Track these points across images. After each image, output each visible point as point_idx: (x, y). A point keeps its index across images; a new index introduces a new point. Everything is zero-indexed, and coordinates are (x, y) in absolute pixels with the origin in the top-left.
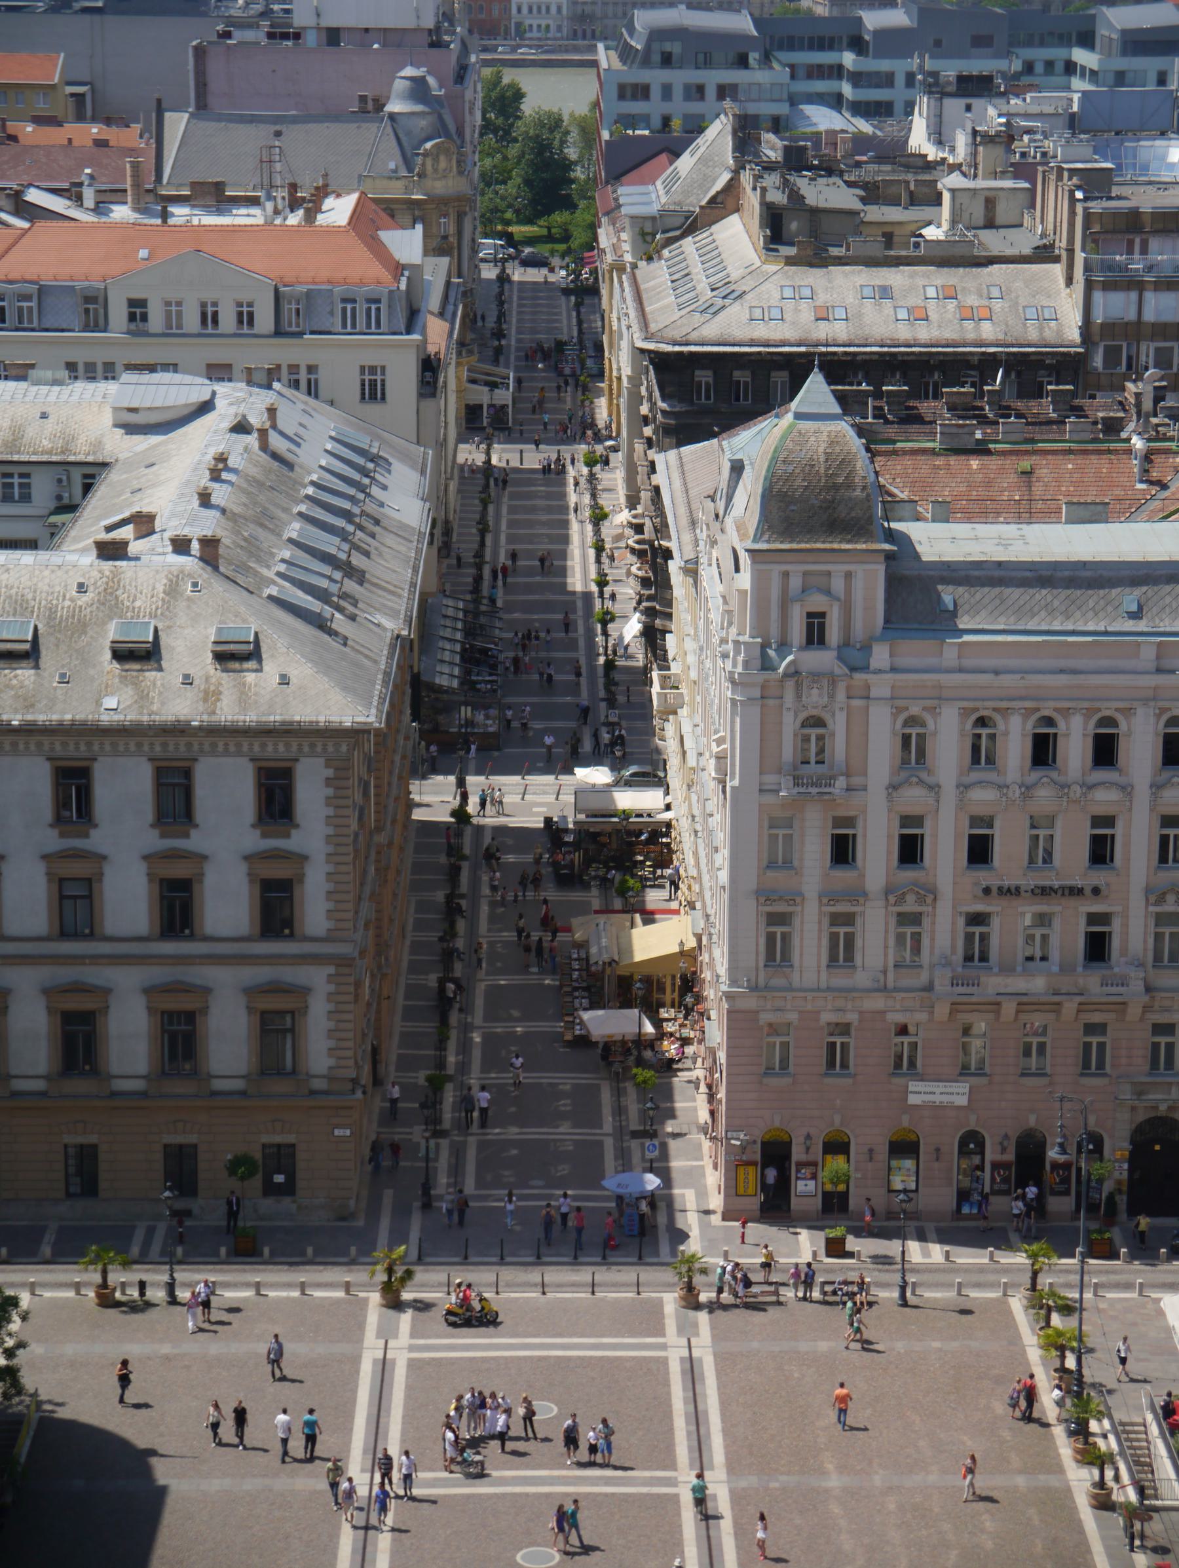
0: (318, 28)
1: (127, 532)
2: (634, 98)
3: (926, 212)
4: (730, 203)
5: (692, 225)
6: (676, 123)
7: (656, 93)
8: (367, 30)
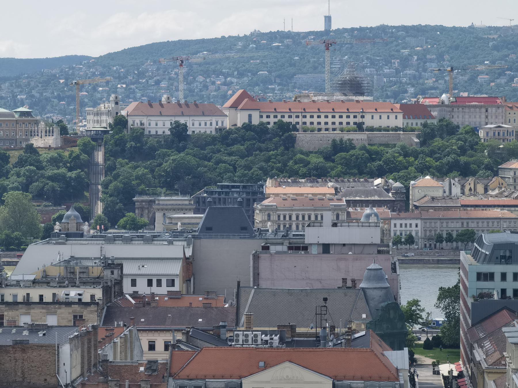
0: (318, 244)
7: (498, 277)
8: (344, 245)
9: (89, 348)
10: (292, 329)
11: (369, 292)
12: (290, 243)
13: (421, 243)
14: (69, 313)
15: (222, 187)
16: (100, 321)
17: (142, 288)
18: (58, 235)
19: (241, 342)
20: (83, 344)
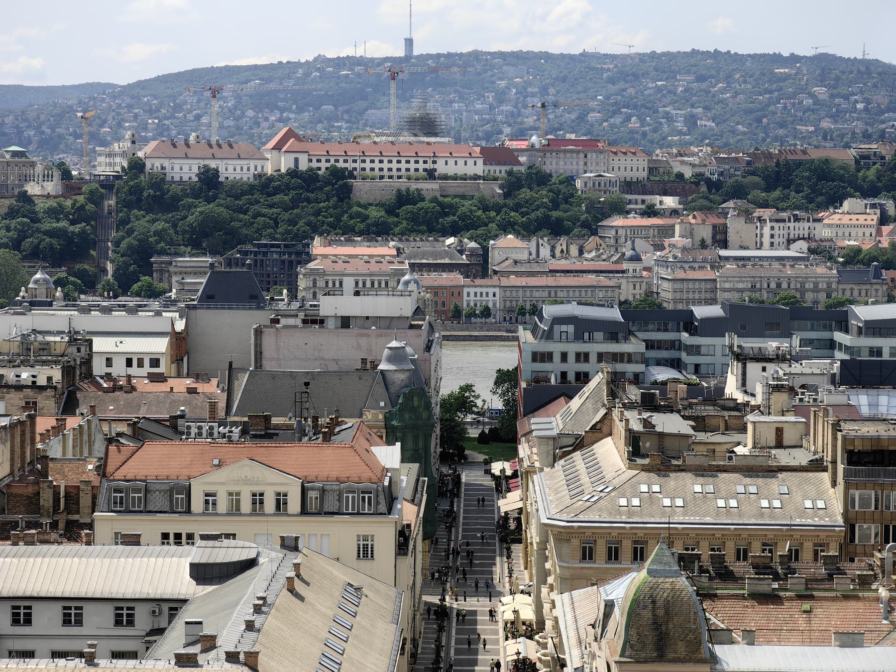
0: (336, 317)
1: (195, 649)
2: (542, 361)
3: (737, 437)
4: (605, 429)
5: (580, 443)
6: (571, 377)
7: (557, 358)
8: (367, 318)
9: (23, 442)
10: (266, 420)
11: (389, 376)
12: (306, 315)
13: (499, 316)
14: (20, 399)
15: (259, 246)
16: (59, 409)
17: (119, 369)
18: (20, 303)
19: (193, 435)
20: (13, 437)
